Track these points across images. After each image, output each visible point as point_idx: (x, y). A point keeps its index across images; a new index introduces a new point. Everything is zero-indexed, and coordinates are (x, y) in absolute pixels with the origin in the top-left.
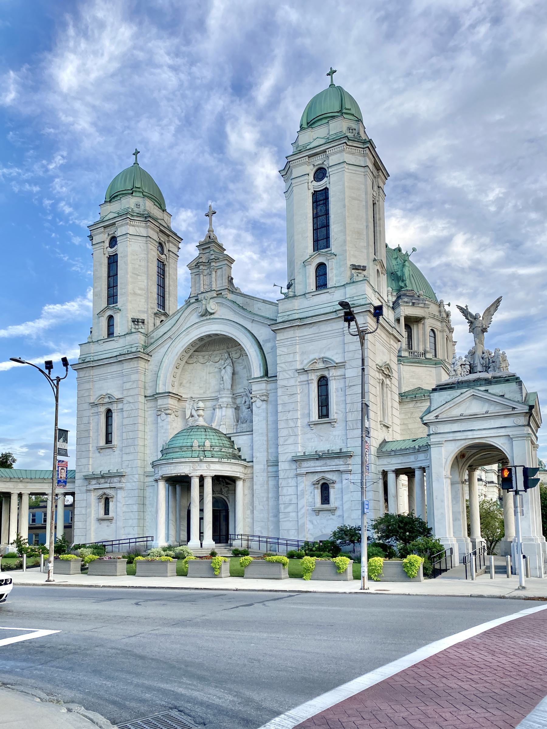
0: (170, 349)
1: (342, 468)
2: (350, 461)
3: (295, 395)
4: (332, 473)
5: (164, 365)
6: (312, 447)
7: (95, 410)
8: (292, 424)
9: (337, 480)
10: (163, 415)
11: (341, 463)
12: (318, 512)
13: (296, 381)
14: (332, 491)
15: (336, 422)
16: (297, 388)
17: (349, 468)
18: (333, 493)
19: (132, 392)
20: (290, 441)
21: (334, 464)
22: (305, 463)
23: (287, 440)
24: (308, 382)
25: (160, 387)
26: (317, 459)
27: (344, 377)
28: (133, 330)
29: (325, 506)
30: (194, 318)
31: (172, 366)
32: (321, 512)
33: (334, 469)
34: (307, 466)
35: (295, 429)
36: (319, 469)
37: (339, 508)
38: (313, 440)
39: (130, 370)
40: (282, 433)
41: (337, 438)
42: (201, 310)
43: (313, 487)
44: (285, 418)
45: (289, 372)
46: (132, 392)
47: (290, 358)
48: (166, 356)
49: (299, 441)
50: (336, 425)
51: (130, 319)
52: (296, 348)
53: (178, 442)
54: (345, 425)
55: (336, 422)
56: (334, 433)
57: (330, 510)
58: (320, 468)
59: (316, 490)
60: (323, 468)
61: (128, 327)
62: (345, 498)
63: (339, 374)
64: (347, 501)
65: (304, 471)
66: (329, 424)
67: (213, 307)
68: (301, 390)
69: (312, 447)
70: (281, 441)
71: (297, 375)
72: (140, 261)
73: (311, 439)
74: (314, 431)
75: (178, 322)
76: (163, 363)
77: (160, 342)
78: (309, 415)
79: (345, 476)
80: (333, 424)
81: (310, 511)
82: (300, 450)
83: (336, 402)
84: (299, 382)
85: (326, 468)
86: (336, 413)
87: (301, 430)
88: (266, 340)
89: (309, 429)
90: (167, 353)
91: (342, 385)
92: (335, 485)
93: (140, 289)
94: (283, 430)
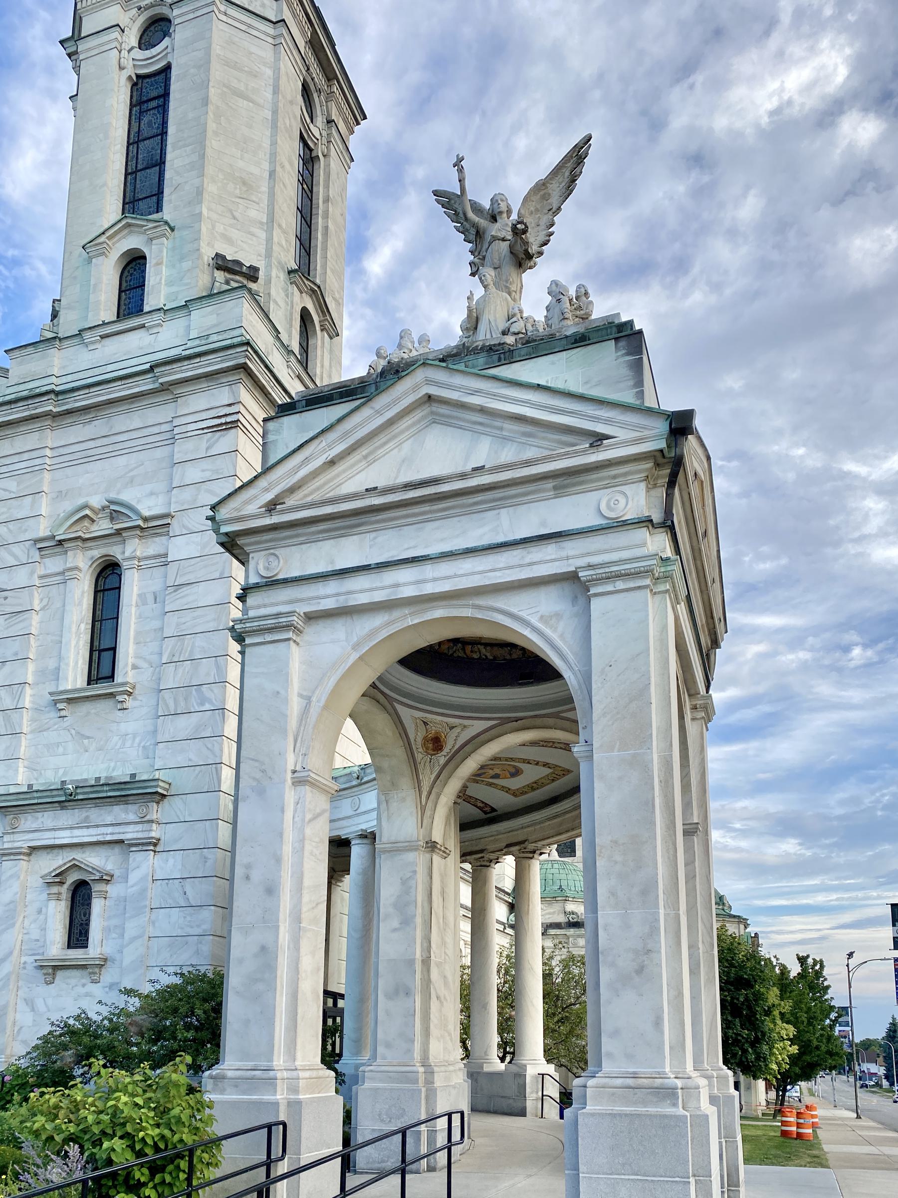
1: (130, 833)
2: (155, 811)
3: (26, 615)
4: (103, 851)
6: (57, 769)
9: (117, 873)
11: (132, 817)
12: (53, 970)
13: (32, 573)
14: (97, 906)
16: (31, 596)
17: (153, 834)
18: (99, 911)
21: (109, 819)
22: (29, 816)
24: (65, 576)
26: (62, 805)
27: (163, 560)
29: (76, 954)
32: (60, 974)
33: (108, 838)
34: (34, 826)
35: (14, 715)
36: (64, 838)
37: (113, 961)
38: (61, 749)
41: (128, 744)
43: (44, 896)
45: (15, 549)
47: (23, 509)
49: (22, 752)
50: (130, 703)
52: (41, 481)
54: (153, 702)
56: (123, 727)
57: (84, 967)
58: (67, 833)
59: (52, 904)
60: (77, 832)
62: (132, 928)
63: (151, 551)
64: (134, 939)
65: (22, 841)
68: (45, 601)
71: (36, 556)
73: (58, 744)
78: (56, 674)
79: (137, 857)
80: (120, 698)
81: (30, 967)
82: (20, 779)
83: (138, 633)
84: (41, 577)
85: (85, 832)
86: (134, 667)
87: (33, 720)
89: (54, 714)
91: (156, 585)
92: (109, 888)
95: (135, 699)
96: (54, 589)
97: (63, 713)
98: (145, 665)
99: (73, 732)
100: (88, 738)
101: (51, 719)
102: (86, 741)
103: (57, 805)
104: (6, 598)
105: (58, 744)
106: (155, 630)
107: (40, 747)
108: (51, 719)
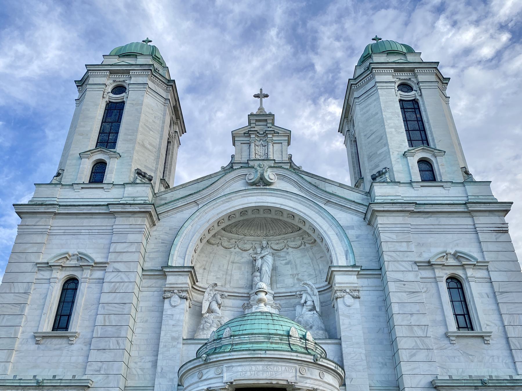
0: (198, 213)
5: (185, 231)
6: (457, 369)
7: (46, 274)
8: (419, 332)
10: (175, 299)
15: (489, 336)
19: (125, 257)
20: (422, 355)
23: (414, 355)
25: (175, 258)
28: (138, 181)
30: (239, 185)
31: (197, 237)
35: (426, 340)
39: (128, 227)
40: (403, 344)
42: (253, 177)
44: (405, 323)
45: (403, 263)
46: (125, 257)
48: (190, 221)
51: (133, 170)
53: (248, 327)
55: (489, 336)
61: (129, 177)
66: (480, 340)
67: (272, 177)
69: (457, 369)
70: (403, 355)
71: (417, 268)
72: (155, 118)
73: (454, 357)
74: (457, 346)
75: (214, 185)
76: (183, 228)
77: (179, 204)
88: (348, 227)
90: (193, 217)
93: (150, 144)
94: (405, 339)
95: (492, 340)
96: (429, 285)
97: (454, 342)
98: (493, 325)
99: (461, 352)
100: (471, 355)
101: (446, 344)
102: (471, 357)
103: (474, 387)
104: (404, 285)
105: (454, 357)
106: (493, 310)
107: (443, 357)
108: (446, 344)
